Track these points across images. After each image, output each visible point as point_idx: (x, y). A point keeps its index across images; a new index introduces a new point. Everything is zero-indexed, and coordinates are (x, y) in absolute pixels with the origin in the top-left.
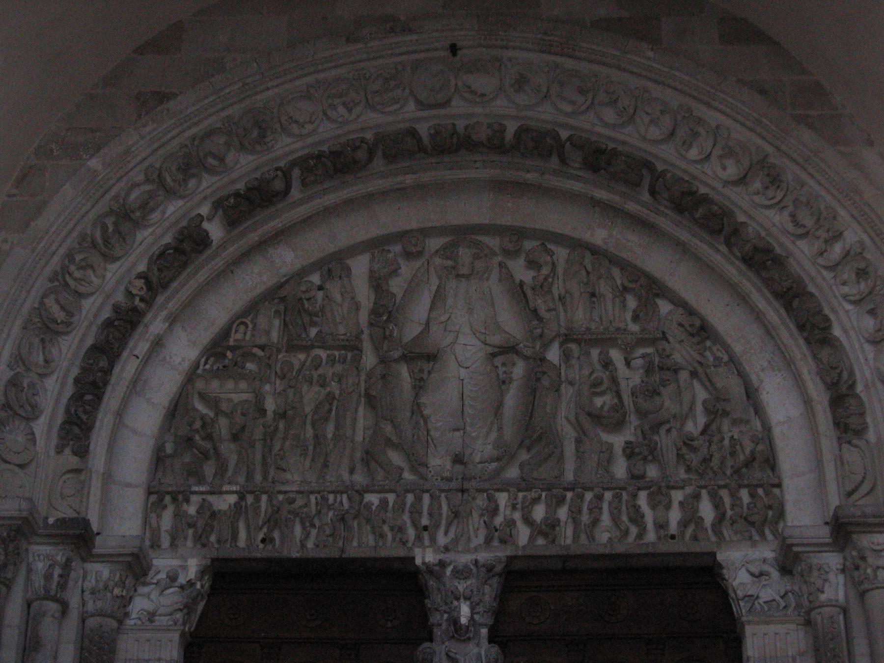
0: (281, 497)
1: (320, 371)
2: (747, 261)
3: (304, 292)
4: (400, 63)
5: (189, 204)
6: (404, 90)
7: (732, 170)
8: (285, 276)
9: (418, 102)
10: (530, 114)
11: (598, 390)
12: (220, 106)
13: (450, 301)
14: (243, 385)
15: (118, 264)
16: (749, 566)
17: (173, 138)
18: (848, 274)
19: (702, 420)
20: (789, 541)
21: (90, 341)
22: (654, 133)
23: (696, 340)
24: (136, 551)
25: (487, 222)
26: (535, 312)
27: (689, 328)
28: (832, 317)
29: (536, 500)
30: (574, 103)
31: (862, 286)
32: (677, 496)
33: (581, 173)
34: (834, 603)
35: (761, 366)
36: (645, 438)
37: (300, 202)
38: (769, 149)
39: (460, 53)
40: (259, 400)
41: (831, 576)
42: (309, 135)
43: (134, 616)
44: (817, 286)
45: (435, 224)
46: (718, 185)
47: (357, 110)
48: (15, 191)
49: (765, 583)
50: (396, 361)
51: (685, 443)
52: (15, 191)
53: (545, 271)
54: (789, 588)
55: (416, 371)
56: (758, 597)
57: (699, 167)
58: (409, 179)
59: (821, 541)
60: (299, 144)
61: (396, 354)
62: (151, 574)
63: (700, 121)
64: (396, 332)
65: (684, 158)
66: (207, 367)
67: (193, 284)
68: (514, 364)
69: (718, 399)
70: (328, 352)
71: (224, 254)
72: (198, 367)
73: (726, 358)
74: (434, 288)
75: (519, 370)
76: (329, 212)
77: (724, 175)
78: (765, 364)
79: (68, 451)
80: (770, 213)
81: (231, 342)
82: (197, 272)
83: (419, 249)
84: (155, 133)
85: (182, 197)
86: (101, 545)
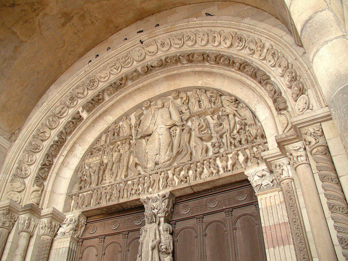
3: (116, 127)
7: (228, 43)
9: (136, 61)
10: (168, 53)
16: (257, 174)
18: (270, 57)
22: (204, 43)
27: (231, 101)
28: (270, 75)
30: (179, 44)
34: (287, 178)
37: (109, 101)
38: (236, 30)
39: (143, 43)
41: (285, 167)
44: (264, 68)
45: (152, 97)
49: (264, 178)
56: (262, 185)
59: (277, 154)
64: (140, 130)
67: (80, 132)
69: (243, 120)
76: (119, 102)
77: (226, 46)
78: (256, 103)
79: (35, 185)
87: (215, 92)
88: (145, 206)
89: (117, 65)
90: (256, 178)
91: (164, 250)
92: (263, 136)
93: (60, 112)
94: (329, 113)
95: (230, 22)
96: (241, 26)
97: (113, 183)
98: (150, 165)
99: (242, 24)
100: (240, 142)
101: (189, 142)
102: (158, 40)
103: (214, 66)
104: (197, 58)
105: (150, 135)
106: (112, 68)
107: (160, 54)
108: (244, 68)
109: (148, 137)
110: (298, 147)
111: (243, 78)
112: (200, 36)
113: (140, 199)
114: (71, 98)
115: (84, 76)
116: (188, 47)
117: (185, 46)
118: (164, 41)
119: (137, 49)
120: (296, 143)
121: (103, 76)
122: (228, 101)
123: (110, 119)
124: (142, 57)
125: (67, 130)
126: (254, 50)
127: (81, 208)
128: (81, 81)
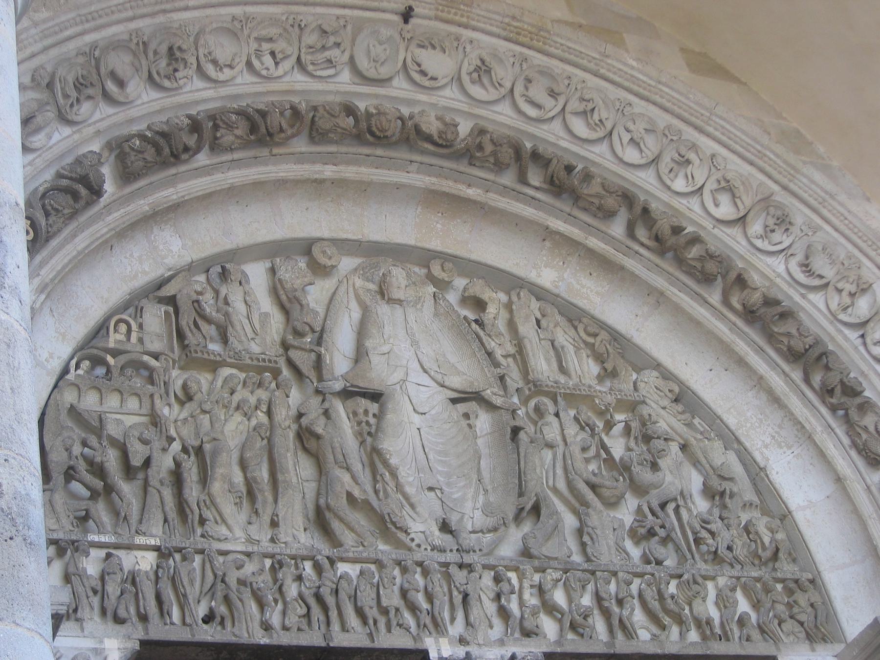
2: (750, 315)
4: (344, 17)
5: (76, 137)
6: (343, 52)
7: (725, 210)
8: (170, 270)
12: (130, 14)
13: (388, 330)
25: (412, 242)
30: (539, 107)
33: (538, 195)
35: (763, 441)
38: (776, 188)
39: (413, 21)
46: (708, 224)
47: (286, 65)
51: (702, 527)
57: (684, 201)
58: (328, 171)
60: (210, 93)
63: (694, 147)
66: (80, 372)
71: (110, 218)
78: (768, 440)
81: (111, 345)
82: (74, 236)
84: (50, 24)
95: (759, 148)
96: (796, 181)
97: (266, 546)
99: (805, 180)
103: (642, 251)
104: (598, 196)
106: (266, 46)
107: (450, 97)
111: (738, 341)
112: (631, 127)
117: (557, 125)
119: (385, 32)
121: (223, 56)
124: (384, 71)
126: (824, 281)
128: (133, 25)
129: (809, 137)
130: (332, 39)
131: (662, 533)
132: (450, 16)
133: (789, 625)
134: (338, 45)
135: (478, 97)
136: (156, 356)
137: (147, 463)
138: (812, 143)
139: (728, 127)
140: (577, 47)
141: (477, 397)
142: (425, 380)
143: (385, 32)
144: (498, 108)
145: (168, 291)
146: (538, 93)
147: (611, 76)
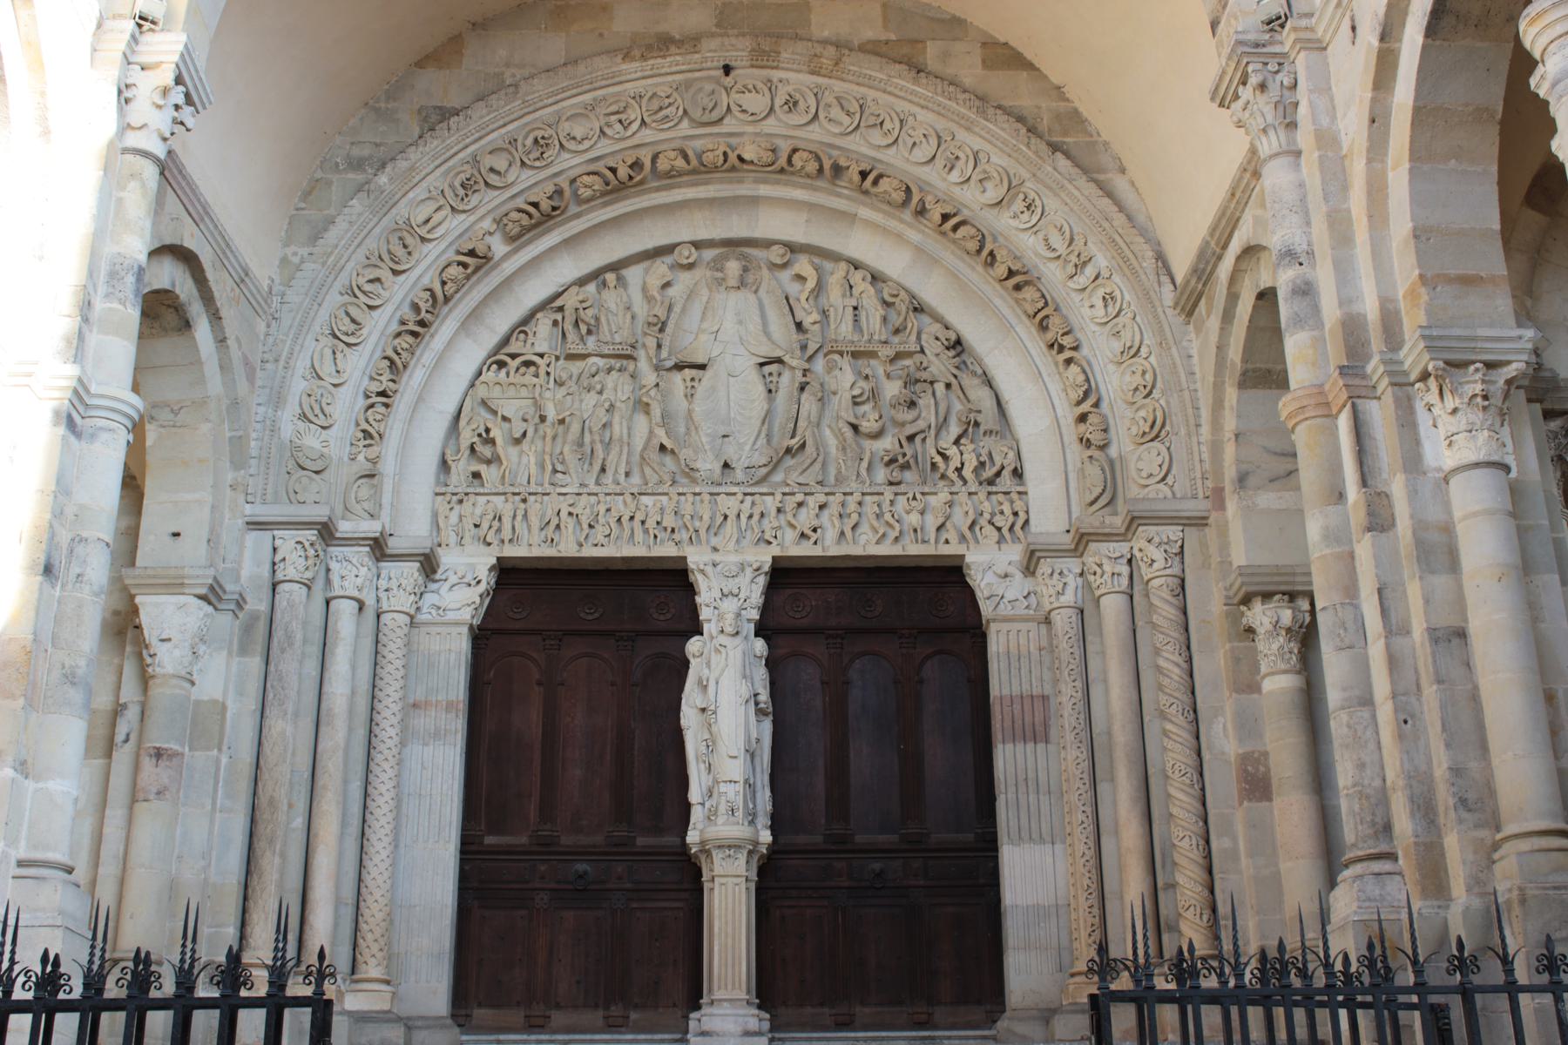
0: (562, 498)
1: (596, 378)
3: (582, 302)
7: (993, 193)
9: (692, 120)
11: (859, 400)
12: (501, 123)
14: (524, 392)
15: (402, 278)
17: (456, 154)
19: (954, 430)
20: (1032, 547)
21: (378, 354)
23: (952, 353)
24: (427, 551)
26: (799, 326)
29: (800, 505)
30: (841, 124)
31: (1110, 309)
32: (932, 500)
36: (901, 446)
37: (577, 216)
38: (1025, 174)
39: (733, 74)
40: (537, 405)
42: (586, 151)
43: (425, 610)
47: (635, 126)
48: (303, 205)
50: (669, 369)
51: (939, 453)
52: (303, 205)
53: (811, 284)
54: (1031, 589)
55: (688, 379)
61: (669, 364)
62: (440, 571)
65: (945, 180)
68: (780, 374)
69: (971, 411)
70: (605, 360)
72: (480, 374)
73: (980, 371)
74: (705, 299)
75: (787, 382)
80: (1024, 236)
83: (691, 260)
85: (464, 211)
86: (394, 545)
87: (903, 293)
88: (701, 582)
89: (629, 111)
90: (990, 578)
91: (762, 705)
92: (1018, 474)
93: (428, 221)
94: (1204, 514)
98: (708, 465)
100: (959, 470)
101: (818, 425)
102: (780, 85)
104: (885, 192)
105: (702, 367)
106: (613, 118)
108: (1018, 288)
109: (694, 372)
110: (1119, 554)
112: (913, 134)
113: (684, 558)
114: (468, 180)
115: (515, 115)
116: (864, 147)
117: (856, 136)
118: (798, 96)
119: (708, 87)
120: (1115, 544)
121: (578, 132)
122: (937, 339)
123: (567, 269)
124: (715, 115)
125: (446, 288)
127: (489, 544)
128: (503, 131)
129: (1085, 114)
130: (667, 101)
131: (901, 460)
132: (765, 63)
133: (989, 529)
134: (670, 104)
135: (792, 123)
136: (541, 356)
137: (524, 434)
138: (1083, 122)
139: (991, 126)
140: (868, 72)
141: (779, 361)
142: (742, 351)
143: (708, 87)
144: (811, 128)
145: (558, 303)
146: (836, 112)
147: (897, 92)
